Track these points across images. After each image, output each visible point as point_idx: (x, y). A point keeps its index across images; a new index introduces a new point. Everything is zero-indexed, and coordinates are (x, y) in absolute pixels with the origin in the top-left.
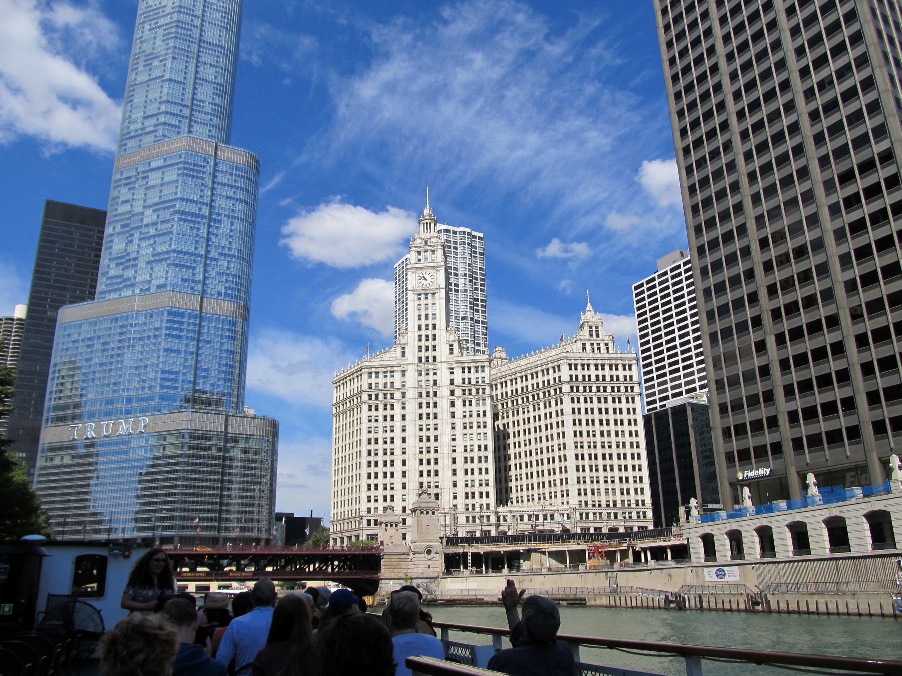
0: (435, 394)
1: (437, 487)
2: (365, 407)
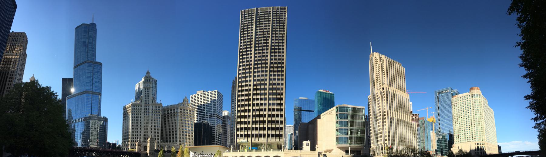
1: (148, 136)
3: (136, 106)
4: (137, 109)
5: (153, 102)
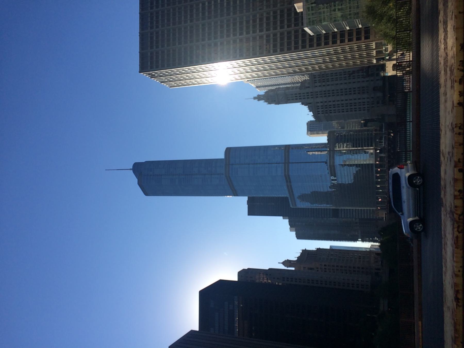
0: (325, 91)
2: (331, 114)
3: (319, 110)
4: (322, 108)
5: (309, 87)
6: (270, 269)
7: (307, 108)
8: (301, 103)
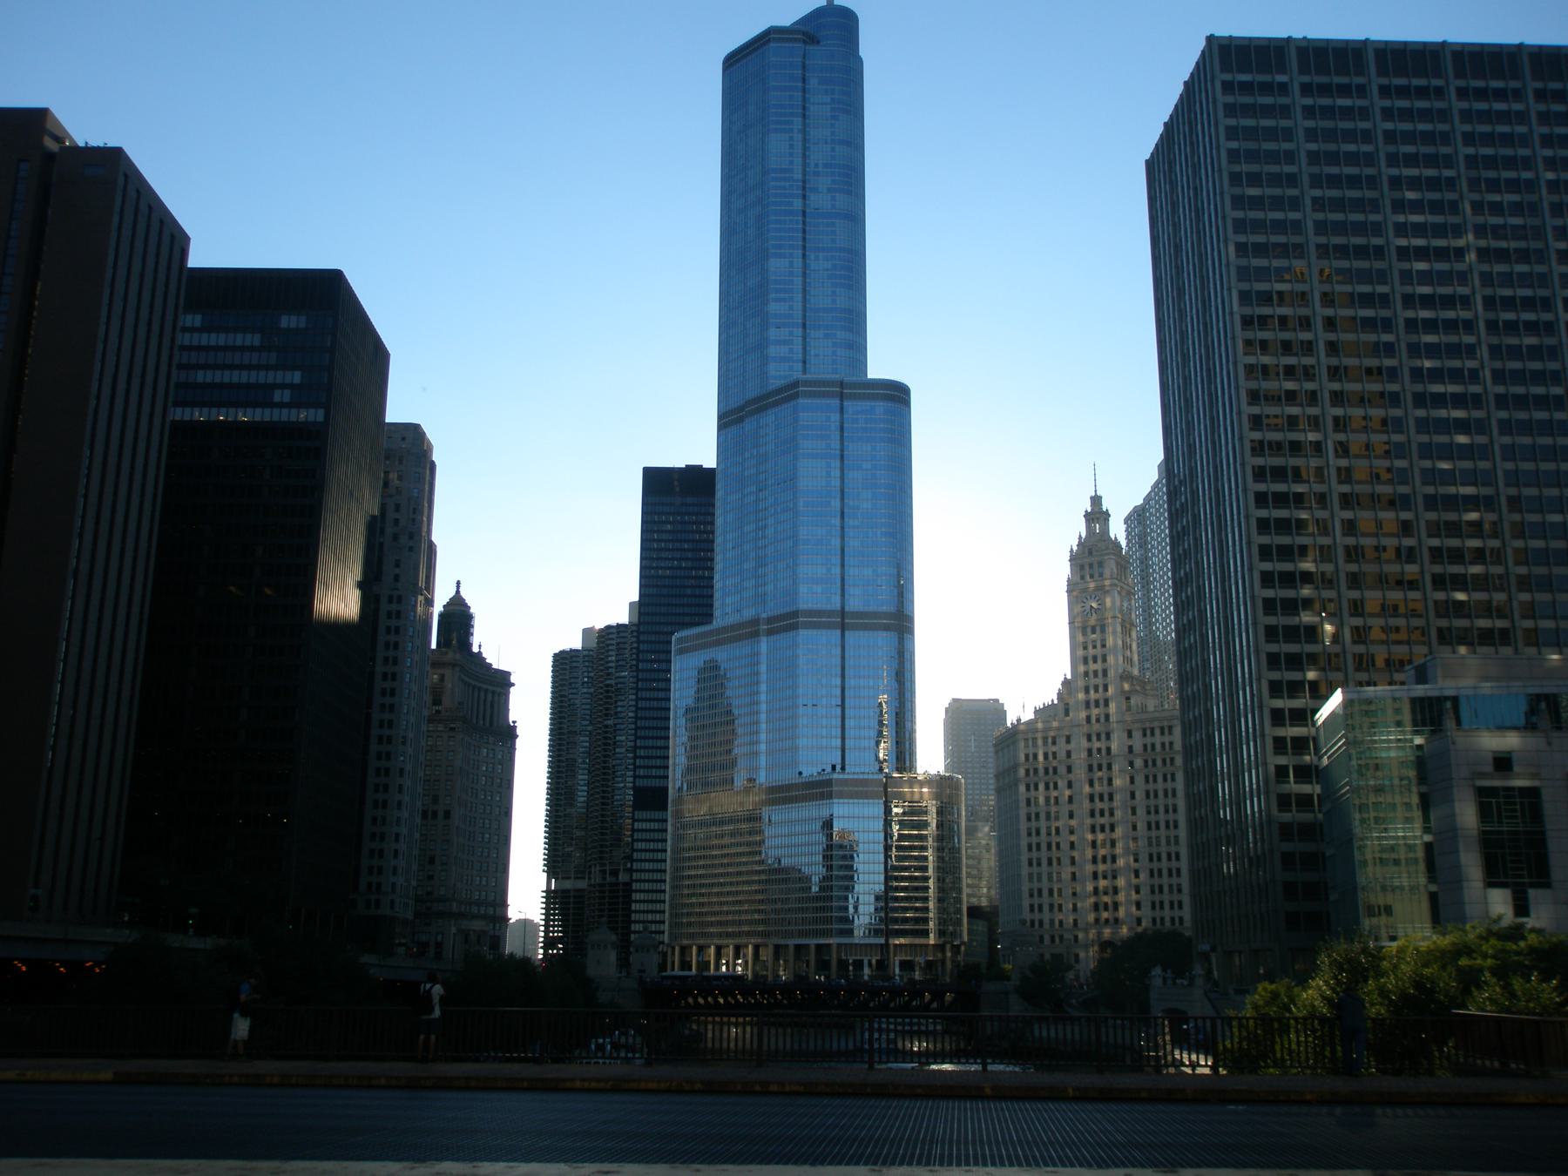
2: (1022, 788)
6: (431, 549)
7: (1048, 701)
8: (1069, 677)
